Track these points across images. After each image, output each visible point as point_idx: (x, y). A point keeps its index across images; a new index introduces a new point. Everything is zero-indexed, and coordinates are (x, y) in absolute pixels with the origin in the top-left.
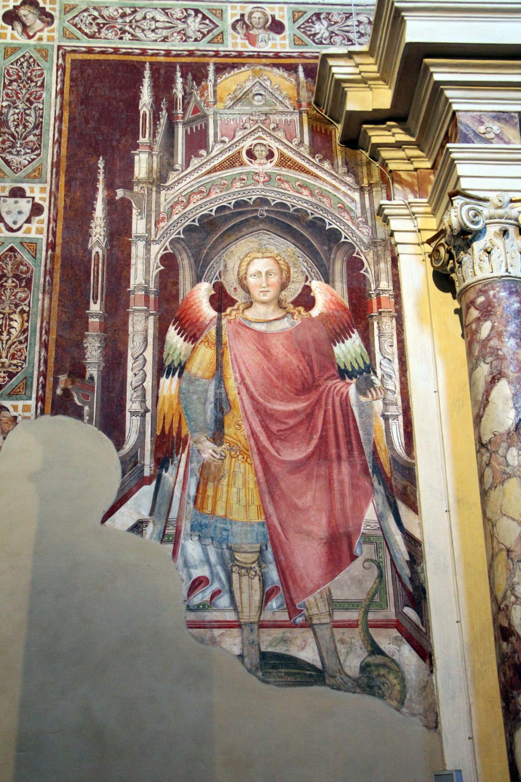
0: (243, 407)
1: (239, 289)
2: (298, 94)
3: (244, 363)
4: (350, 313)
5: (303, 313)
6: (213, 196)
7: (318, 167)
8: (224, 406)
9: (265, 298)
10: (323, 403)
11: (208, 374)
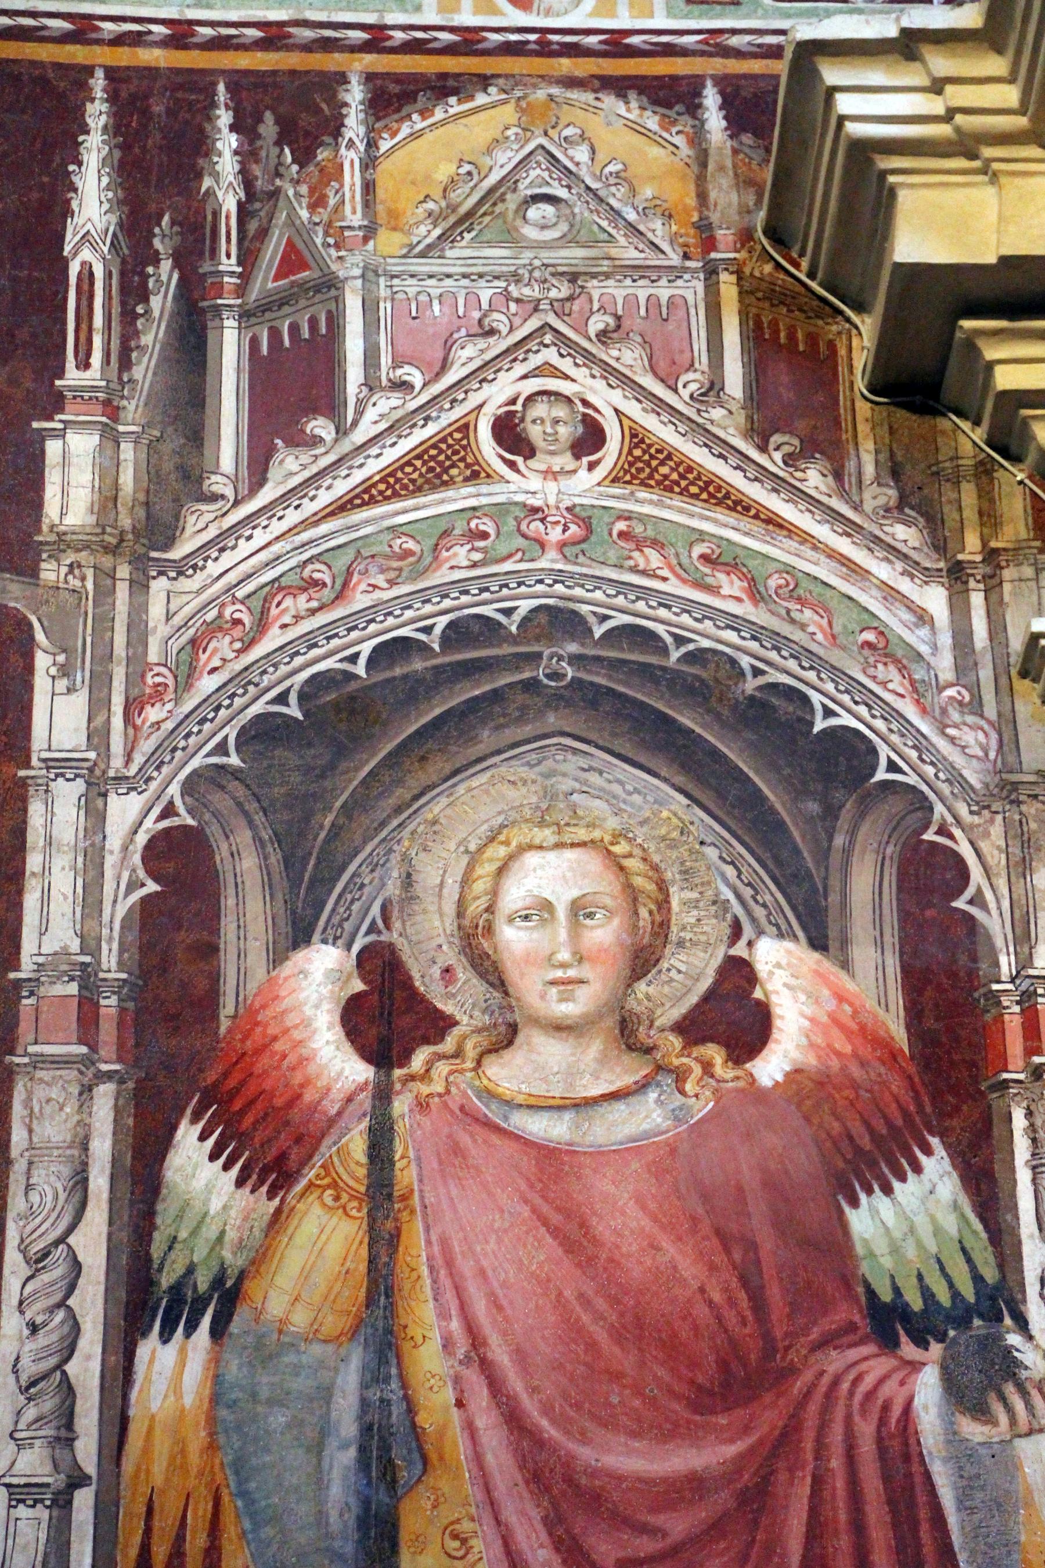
0: (478, 1459)
1: (463, 974)
2: (702, 196)
3: (482, 1273)
4: (912, 1070)
5: (720, 1068)
6: (360, 600)
7: (778, 485)
8: (398, 1453)
9: (568, 1009)
10: (809, 1445)
11: (331, 1324)
